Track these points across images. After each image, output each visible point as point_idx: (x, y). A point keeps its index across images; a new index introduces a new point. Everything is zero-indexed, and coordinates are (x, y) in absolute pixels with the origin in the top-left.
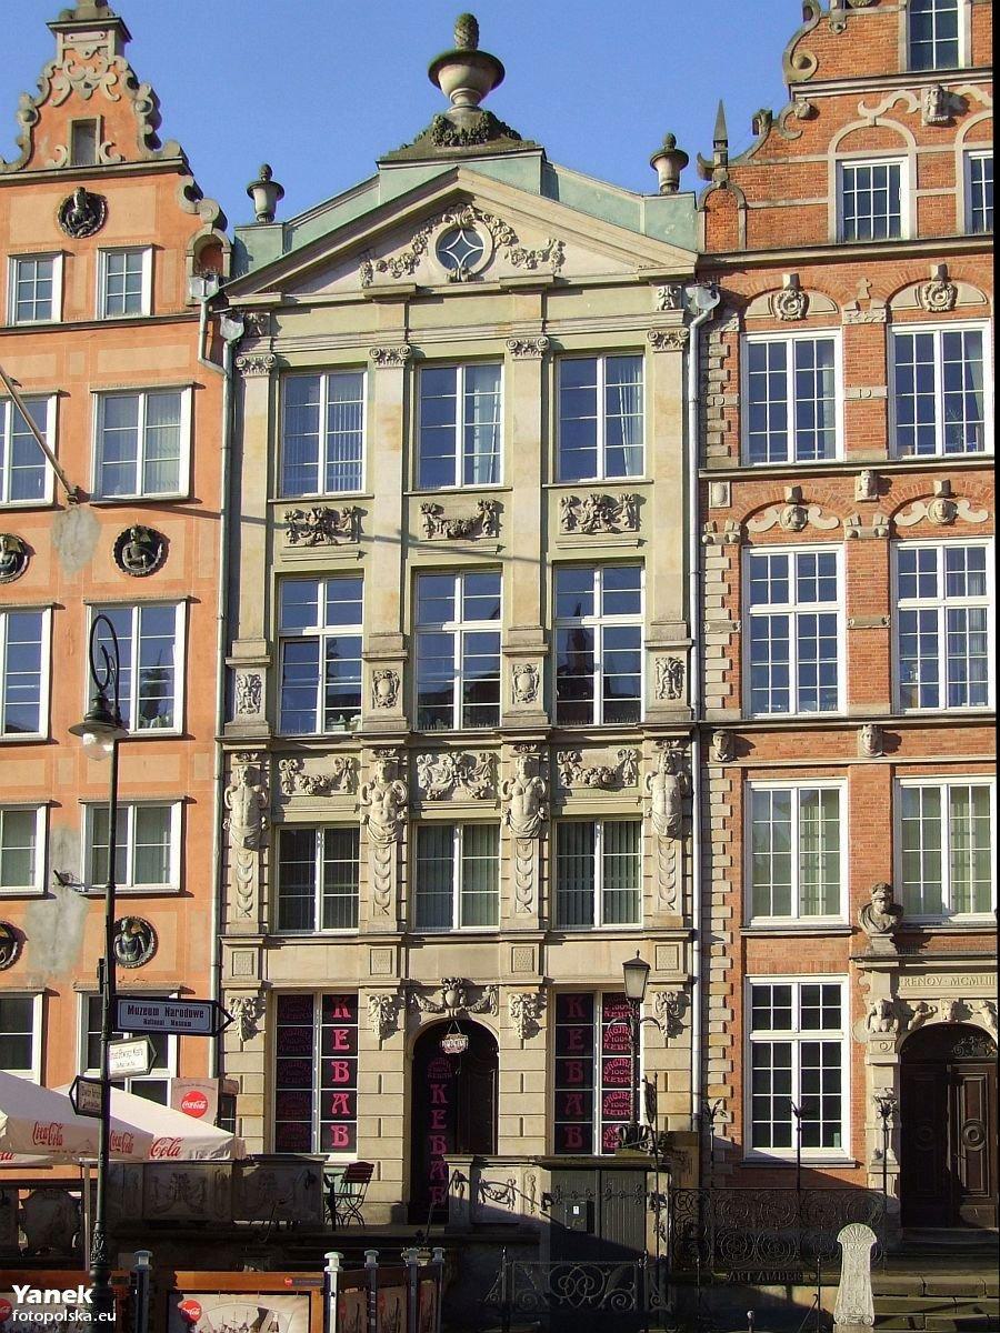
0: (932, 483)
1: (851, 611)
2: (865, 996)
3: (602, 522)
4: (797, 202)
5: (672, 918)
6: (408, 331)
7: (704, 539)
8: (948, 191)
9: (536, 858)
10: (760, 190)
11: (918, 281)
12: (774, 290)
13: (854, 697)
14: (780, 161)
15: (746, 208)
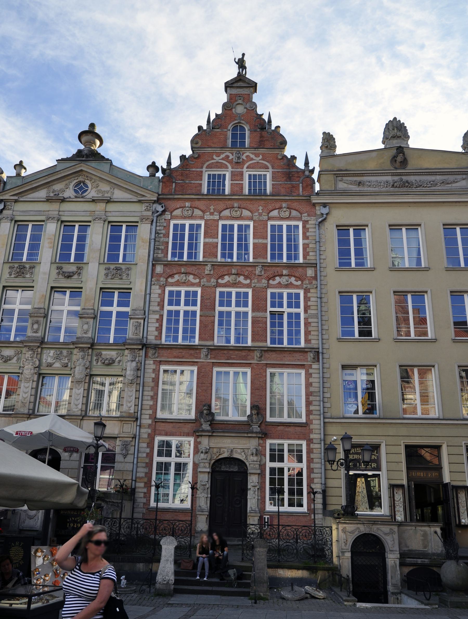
2: (199, 446)
4: (192, 182)
6: (59, 211)
7: (153, 283)
8: (241, 182)
9: (82, 389)
10: (180, 178)
13: (200, 339)
15: (176, 183)
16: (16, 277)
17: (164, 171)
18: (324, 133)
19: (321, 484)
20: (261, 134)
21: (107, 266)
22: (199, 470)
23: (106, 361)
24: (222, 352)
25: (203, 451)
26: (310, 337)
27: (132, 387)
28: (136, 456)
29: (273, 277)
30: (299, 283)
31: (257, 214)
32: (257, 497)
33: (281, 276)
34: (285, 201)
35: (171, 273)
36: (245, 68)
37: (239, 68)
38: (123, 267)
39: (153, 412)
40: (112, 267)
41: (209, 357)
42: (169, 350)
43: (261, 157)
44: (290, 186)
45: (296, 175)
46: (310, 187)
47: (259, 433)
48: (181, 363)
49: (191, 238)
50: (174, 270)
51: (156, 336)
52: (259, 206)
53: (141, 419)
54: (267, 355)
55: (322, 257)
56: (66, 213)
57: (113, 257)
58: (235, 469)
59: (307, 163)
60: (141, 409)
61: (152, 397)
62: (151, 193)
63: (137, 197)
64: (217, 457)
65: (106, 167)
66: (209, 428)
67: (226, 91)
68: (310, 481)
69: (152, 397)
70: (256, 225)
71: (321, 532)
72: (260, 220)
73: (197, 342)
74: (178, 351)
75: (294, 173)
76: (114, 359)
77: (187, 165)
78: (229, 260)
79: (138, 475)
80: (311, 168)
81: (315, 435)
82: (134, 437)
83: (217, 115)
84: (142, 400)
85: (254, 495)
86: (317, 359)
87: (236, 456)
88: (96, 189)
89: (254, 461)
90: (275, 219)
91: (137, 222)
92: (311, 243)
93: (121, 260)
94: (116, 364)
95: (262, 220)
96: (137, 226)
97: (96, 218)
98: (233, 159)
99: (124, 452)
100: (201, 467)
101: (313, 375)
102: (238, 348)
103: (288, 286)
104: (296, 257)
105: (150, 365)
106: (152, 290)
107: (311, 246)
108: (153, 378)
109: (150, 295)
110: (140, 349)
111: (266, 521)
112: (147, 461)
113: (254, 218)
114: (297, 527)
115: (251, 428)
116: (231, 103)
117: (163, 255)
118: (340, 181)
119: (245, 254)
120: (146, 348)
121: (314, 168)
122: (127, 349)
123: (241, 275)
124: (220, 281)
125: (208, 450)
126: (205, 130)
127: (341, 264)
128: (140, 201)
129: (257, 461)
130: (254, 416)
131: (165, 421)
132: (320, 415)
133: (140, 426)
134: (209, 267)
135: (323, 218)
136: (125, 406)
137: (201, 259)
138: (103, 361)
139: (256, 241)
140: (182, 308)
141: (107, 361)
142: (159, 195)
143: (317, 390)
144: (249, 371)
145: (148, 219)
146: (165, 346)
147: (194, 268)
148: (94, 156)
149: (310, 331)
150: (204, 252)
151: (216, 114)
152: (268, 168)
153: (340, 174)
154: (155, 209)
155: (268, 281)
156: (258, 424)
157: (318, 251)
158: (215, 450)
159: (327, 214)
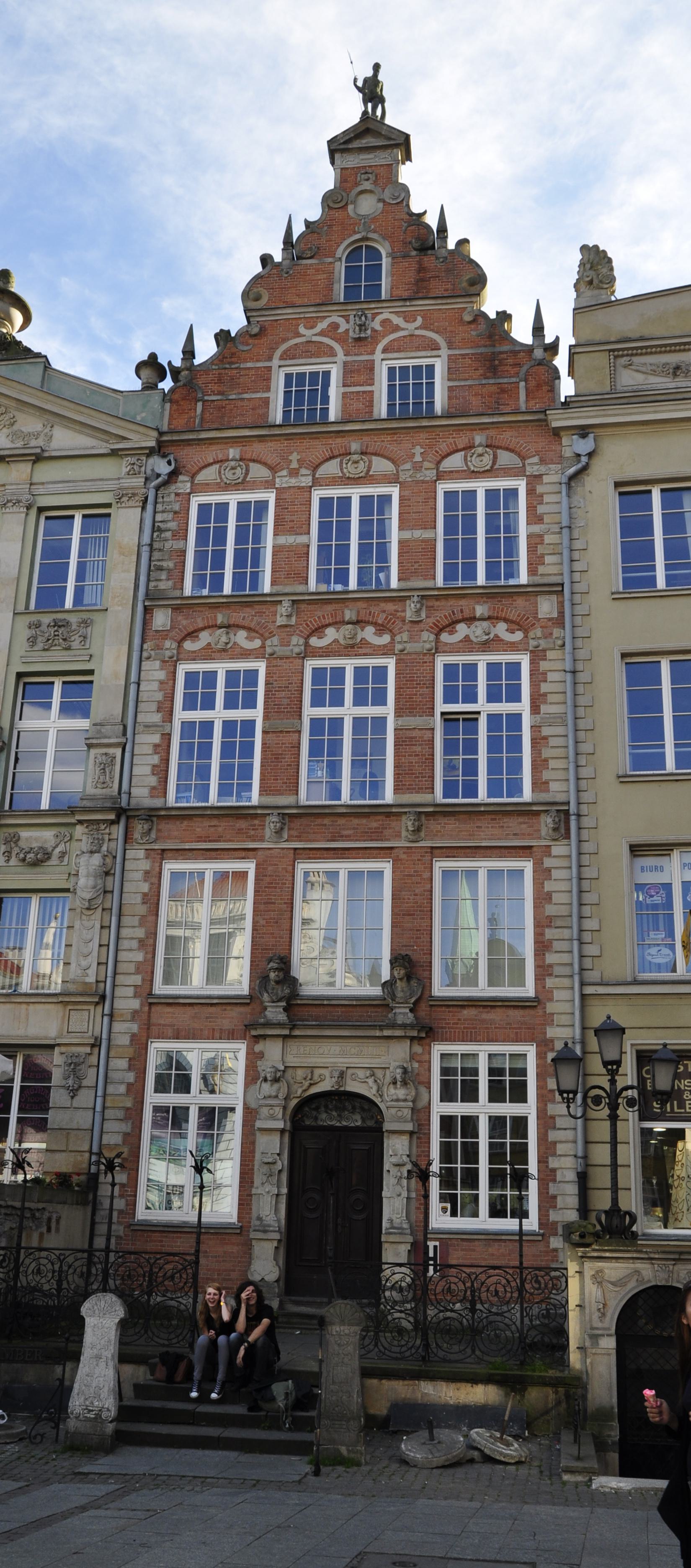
0: (343, 612)
1: (266, 717)
2: (259, 1063)
3: (61, 641)
4: (246, 396)
5: (86, 983)
7: (145, 654)
10: (216, 388)
11: (340, 455)
12: (221, 461)
13: (263, 790)
14: (233, 366)
15: (204, 401)
17: (176, 373)
18: (584, 248)
19: (575, 1156)
20: (420, 263)
21: (34, 618)
22: (259, 1124)
23: (31, 856)
24: (319, 821)
25: (268, 1075)
26: (546, 775)
27: (93, 917)
28: (100, 1093)
29: (449, 625)
30: (518, 636)
31: (408, 466)
32: (405, 1194)
33: (471, 620)
34: (482, 427)
35: (191, 629)
36: (382, 100)
37: (365, 103)
38: (73, 619)
39: (143, 980)
40: (46, 619)
41: (285, 836)
42: (185, 823)
43: (419, 320)
44: (494, 389)
45: (510, 361)
46: (545, 388)
47: (412, 1026)
48: (214, 853)
49: (241, 535)
50: (199, 620)
51: (153, 788)
53: (113, 997)
54: (433, 825)
55: (577, 566)
57: (50, 597)
58: (356, 1121)
59: (538, 329)
60: (115, 973)
61: (141, 941)
62: (141, 429)
63: (107, 442)
64: (305, 1091)
65: (32, 374)
66: (282, 1017)
67: (333, 163)
68: (547, 1149)
69: (141, 941)
70: (406, 493)
71: (538, 1282)
72: (417, 482)
73: (255, 797)
74: (207, 823)
75: (505, 356)
76: (50, 850)
77: (233, 355)
78: (339, 587)
79: (106, 1140)
80: (549, 340)
81: (558, 1030)
82: (96, 1044)
83: (308, 224)
84: (117, 950)
85: (398, 1188)
86: (562, 829)
87: (352, 1086)
88: (10, 431)
89: (398, 1100)
90: (455, 475)
91: (109, 505)
92: (548, 531)
93: (69, 603)
94: (54, 861)
95: (423, 482)
96: (109, 515)
97: (8, 501)
98: (347, 331)
99: (70, 1082)
100: (263, 1116)
101: (555, 874)
102: (359, 811)
103: (488, 645)
104: (511, 572)
105: (138, 860)
106: (142, 673)
107: (548, 539)
108: (145, 895)
109: (139, 685)
110: (113, 822)
111: (431, 1254)
112: (129, 1104)
113: (402, 477)
114: (473, 1270)
115: (390, 1015)
116: (345, 190)
117: (170, 583)
118: (625, 367)
119: (380, 570)
120: (128, 818)
121: (557, 338)
122: (80, 822)
123: (368, 623)
124: (314, 641)
125: (279, 1074)
126: (279, 264)
127: (628, 583)
128: (114, 453)
129: (405, 1100)
130: (399, 983)
131: (173, 1002)
132: (572, 976)
133: (111, 1016)
134: (284, 608)
135: (580, 466)
136: (73, 966)
137: (267, 588)
138: (22, 856)
139: (407, 535)
140: (219, 714)
141: (32, 855)
142: (161, 434)
143: (563, 911)
144: (386, 867)
145: (134, 495)
146: (173, 813)
147: (248, 612)
148: (5, 349)
149: (546, 760)
150: (274, 571)
151: (306, 221)
152: (436, 347)
153: (624, 350)
154: (153, 470)
155: (437, 635)
156: (410, 1005)
157: (566, 553)
158: (300, 1073)
159: (590, 455)
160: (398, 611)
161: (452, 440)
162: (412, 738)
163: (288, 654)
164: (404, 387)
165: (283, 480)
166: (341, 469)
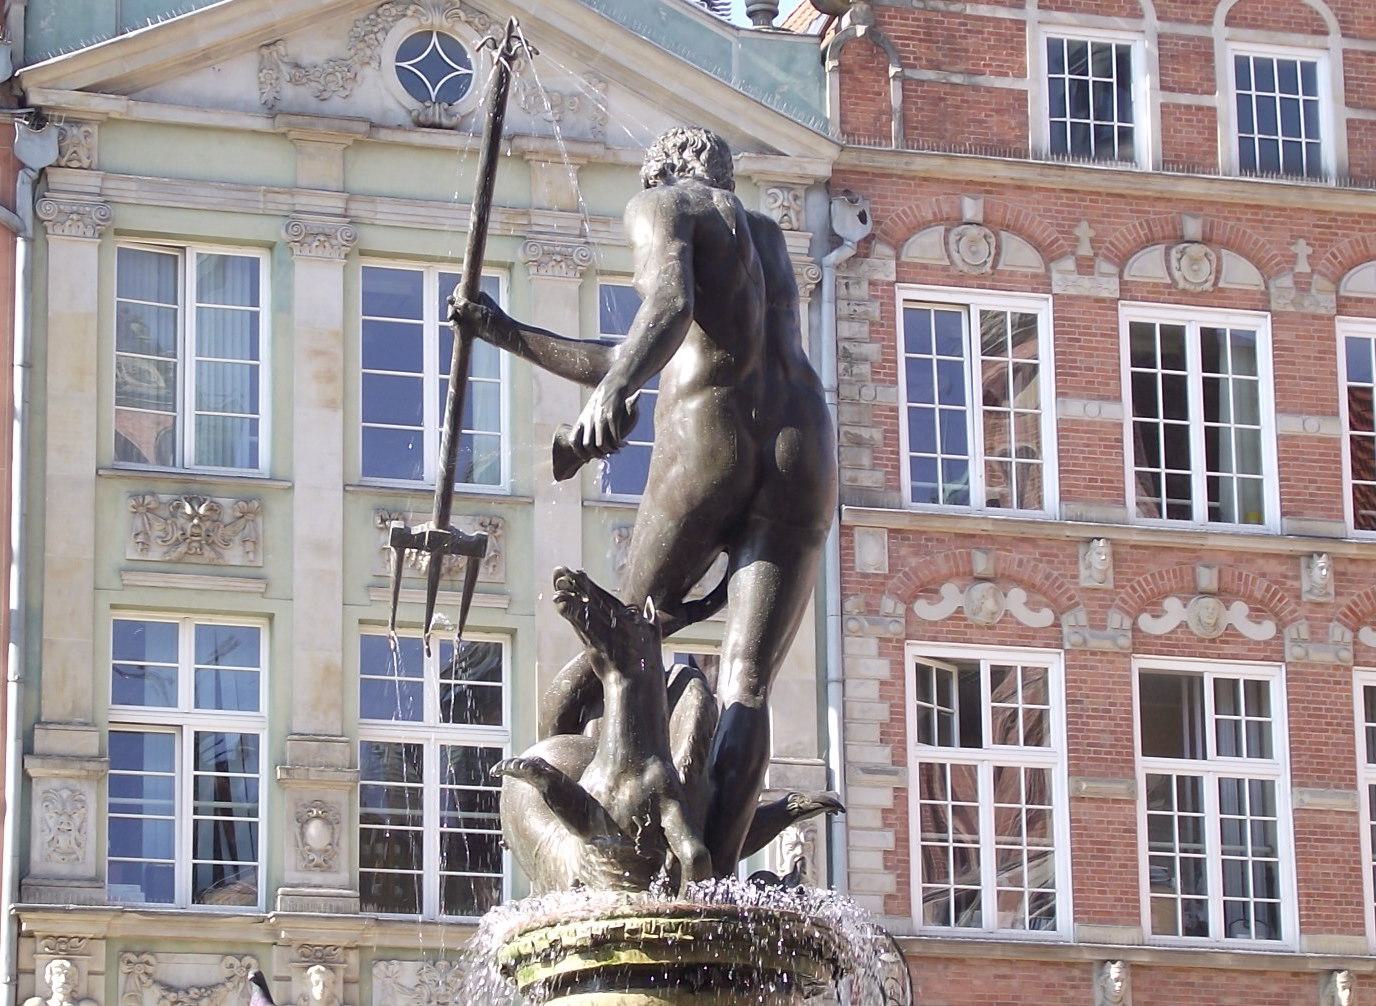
0: (1194, 569)
1: (1075, 770)
7: (852, 625)
10: (922, 49)
16: (178, 561)
31: (1286, 281)
35: (925, 574)
50: (940, 559)
52: (1295, 237)
56: (385, 212)
72: (1304, 316)
74: (991, 971)
95: (1315, 317)
109: (843, 682)
124: (1146, 622)
139: (1294, 425)
150: (1063, 471)
155: (1356, 630)
160: (1286, 577)
161: (1358, 235)
162: (1326, 827)
163: (1107, 645)
164: (1266, 105)
165: (1065, 278)
166: (1168, 268)
